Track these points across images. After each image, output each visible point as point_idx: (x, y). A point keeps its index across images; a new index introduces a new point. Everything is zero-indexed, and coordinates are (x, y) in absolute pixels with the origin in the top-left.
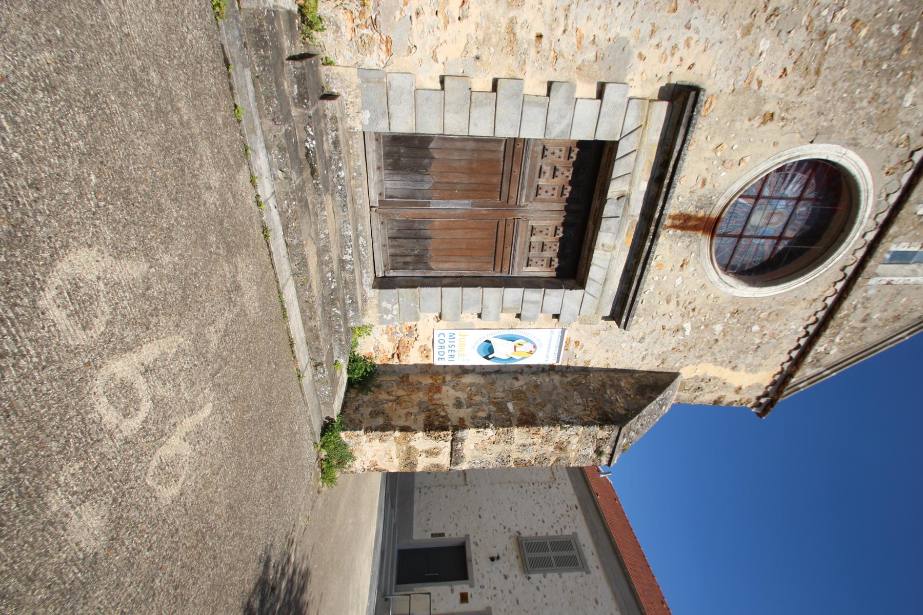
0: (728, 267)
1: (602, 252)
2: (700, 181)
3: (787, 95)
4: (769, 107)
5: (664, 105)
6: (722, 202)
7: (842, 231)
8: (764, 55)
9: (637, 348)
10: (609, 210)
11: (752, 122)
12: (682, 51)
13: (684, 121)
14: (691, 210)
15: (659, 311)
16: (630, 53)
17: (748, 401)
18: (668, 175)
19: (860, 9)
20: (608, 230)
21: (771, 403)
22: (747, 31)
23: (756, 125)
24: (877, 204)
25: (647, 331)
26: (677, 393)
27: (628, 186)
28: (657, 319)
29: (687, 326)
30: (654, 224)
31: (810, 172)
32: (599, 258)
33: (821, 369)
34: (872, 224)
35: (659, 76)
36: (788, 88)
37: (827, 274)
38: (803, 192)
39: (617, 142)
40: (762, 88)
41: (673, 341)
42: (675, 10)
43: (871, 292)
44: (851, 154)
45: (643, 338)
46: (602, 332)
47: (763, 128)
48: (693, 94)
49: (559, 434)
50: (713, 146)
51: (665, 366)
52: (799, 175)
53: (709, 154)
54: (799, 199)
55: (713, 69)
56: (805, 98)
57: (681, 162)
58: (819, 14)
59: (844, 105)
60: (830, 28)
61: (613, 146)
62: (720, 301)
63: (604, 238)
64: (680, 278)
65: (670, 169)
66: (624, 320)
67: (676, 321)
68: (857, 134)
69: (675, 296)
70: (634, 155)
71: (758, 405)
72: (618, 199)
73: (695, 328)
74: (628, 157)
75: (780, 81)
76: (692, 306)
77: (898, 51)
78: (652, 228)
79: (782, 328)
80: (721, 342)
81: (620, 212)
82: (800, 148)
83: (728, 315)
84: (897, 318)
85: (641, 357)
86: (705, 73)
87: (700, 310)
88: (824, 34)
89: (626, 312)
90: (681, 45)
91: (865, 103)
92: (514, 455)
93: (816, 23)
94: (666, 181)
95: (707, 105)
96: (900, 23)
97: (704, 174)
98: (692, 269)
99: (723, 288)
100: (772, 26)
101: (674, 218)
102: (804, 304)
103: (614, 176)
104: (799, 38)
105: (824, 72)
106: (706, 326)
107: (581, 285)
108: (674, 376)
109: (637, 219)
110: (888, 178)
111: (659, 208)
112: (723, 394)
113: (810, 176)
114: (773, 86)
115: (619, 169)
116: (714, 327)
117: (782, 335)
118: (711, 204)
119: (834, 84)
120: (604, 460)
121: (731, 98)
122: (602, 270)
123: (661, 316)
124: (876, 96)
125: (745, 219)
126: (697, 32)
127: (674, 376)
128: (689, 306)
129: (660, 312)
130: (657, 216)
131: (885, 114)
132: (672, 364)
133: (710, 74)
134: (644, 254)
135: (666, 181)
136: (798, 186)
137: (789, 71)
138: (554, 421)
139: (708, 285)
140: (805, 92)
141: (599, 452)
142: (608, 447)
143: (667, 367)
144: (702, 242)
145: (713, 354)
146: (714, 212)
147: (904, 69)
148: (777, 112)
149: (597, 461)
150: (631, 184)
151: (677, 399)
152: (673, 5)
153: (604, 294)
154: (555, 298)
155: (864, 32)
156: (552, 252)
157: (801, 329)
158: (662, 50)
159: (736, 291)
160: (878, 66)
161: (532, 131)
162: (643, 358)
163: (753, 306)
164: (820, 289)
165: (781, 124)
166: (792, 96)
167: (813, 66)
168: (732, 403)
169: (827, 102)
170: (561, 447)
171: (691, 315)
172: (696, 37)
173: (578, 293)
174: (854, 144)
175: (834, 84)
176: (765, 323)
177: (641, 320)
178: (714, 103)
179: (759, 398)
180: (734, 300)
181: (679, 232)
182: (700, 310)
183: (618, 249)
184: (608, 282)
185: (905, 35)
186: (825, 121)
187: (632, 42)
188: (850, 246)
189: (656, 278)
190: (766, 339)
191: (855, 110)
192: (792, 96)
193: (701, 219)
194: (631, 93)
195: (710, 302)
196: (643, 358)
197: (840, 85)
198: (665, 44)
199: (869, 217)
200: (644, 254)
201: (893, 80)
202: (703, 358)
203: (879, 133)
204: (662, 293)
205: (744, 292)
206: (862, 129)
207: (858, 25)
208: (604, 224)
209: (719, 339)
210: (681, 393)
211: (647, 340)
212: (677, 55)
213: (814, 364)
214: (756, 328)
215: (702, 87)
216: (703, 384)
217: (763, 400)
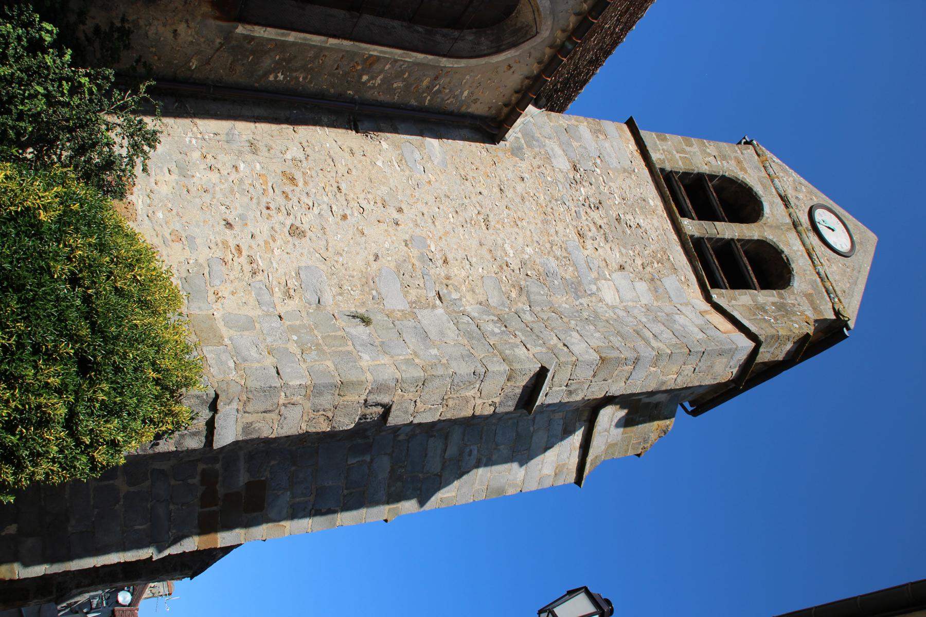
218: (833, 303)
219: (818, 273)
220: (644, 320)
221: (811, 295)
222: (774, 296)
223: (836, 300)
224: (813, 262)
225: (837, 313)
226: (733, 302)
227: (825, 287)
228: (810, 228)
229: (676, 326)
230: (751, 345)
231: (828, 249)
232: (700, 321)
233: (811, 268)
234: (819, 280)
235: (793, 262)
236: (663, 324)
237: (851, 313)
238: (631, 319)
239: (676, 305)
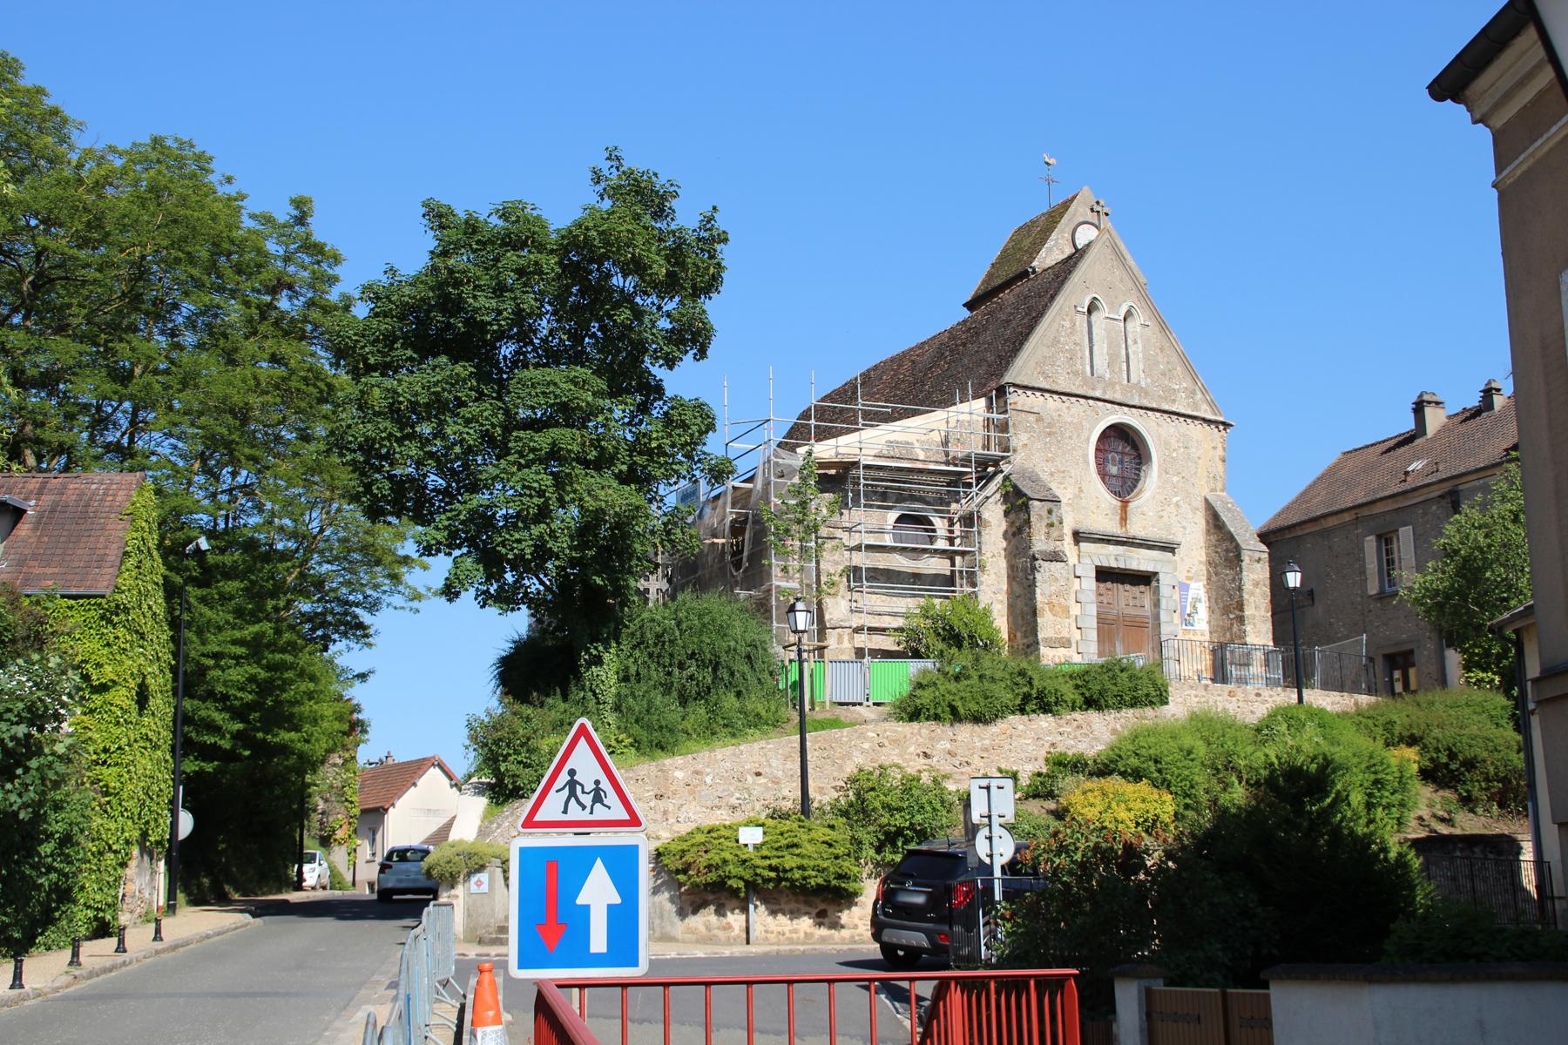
10: (1123, 566)
21: (1223, 423)
24: (1112, 413)
49: (1248, 586)
61: (1097, 568)
67: (1172, 509)
73: (1176, 494)
77: (1054, 433)
84: (1162, 350)
92: (1263, 613)
108: (1206, 500)
115: (1105, 564)
127: (1206, 500)
138: (1240, 589)
143: (1201, 505)
151: (1222, 490)
154: (1165, 590)
156: (1136, 590)
161: (1093, 610)
166: (1073, 481)
170: (1256, 584)
173: (1161, 576)
174: (1088, 439)
185: (1050, 434)
192: (1073, 481)
211: (1184, 524)
213: (1196, 407)
217: (1221, 427)
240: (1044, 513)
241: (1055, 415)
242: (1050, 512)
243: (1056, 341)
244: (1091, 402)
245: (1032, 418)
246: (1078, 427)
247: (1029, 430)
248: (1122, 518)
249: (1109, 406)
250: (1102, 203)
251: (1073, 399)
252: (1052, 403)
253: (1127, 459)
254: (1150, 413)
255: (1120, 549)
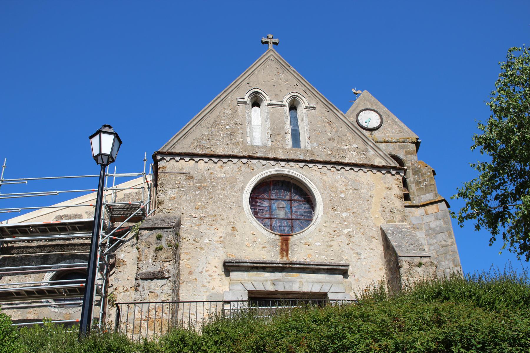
0: (309, 220)
1: (304, 287)
2: (264, 249)
3: (224, 225)
4: (230, 230)
5: (231, 274)
6: (273, 236)
7: (282, 176)
8: (210, 239)
9: (365, 255)
11: (236, 235)
12: (211, 273)
13: (237, 265)
14: (278, 249)
15: (338, 249)
16: (212, 294)
17: (397, 180)
18: (261, 265)
19: (192, 208)
20: (291, 286)
22: (202, 249)
23: (237, 233)
24: (268, 168)
25: (352, 252)
26: (397, 223)
27: (268, 282)
28: (343, 249)
29: (346, 231)
30: (285, 266)
31: (256, 200)
32: (307, 288)
33: (368, 147)
34: (277, 166)
35: (220, 279)
36: (222, 225)
37: (305, 173)
38: (266, 199)
39: (248, 291)
40: (222, 236)
41: (357, 236)
42: (196, 279)
43: (315, 144)
44: (246, 189)
45: (357, 253)
46: (356, 277)
47: (238, 230)
48: (227, 264)
50: (247, 249)
51: (376, 236)
52: (258, 204)
53: (251, 249)
54: (270, 199)
55: (216, 258)
56: (225, 218)
57: (255, 262)
58: (194, 223)
59: (227, 200)
60: (199, 217)
61: (250, 293)
62: (327, 219)
63: (295, 288)
64: (316, 244)
65: (258, 265)
66: (343, 268)
68: (238, 190)
69: (327, 243)
70: (253, 283)
71: (398, 173)
72: (274, 285)
73: (347, 227)
74: (255, 285)
75: (219, 230)
76: (333, 233)
77: (205, 188)
78: (287, 266)
79: (340, 182)
80: (354, 210)
81: (281, 283)
82: (245, 211)
83: (336, 212)
84: (330, 123)
85: (371, 251)
86: (218, 261)
87: (334, 228)
88: (201, 219)
89: (337, 268)
90: (208, 273)
91: (225, 192)
93: (198, 223)
94: (264, 265)
95: (231, 256)
96: (195, 192)
97: (261, 248)
98: (310, 240)
99: (319, 220)
100: (199, 239)
101: (282, 256)
102: (324, 177)
103: (264, 290)
104: (203, 228)
105: (215, 213)
106: (345, 221)
107: (325, 294)
108: (381, 229)
109: (284, 273)
110: (255, 169)
111: (277, 265)
112: (393, 196)
113: (258, 199)
114: (221, 232)
115: (260, 288)
116: (344, 217)
117: (345, 180)
118: (274, 241)
119: (219, 207)
120: (424, 260)
121: (227, 247)
122: (314, 285)
123: (341, 247)
124: (223, 189)
125: (282, 221)
126: (203, 268)
127: (381, 229)
128: (333, 234)
129: (338, 248)
130: (281, 265)
131: (229, 182)
132: (375, 232)
133: (219, 259)
134: (302, 266)
135: (264, 265)
136: (263, 202)
137: (215, 227)
139: (318, 229)
140: (223, 218)
141: (420, 265)
142: (415, 260)
144: (294, 239)
145: (364, 211)
146: (278, 238)
147: (211, 183)
148: (232, 226)
149: (427, 264)
150: (266, 281)
152: (194, 280)
153: (329, 281)
155: (200, 204)
157: (340, 172)
158: (210, 281)
159: (320, 214)
160: (211, 193)
162: (372, 249)
163: (328, 202)
164: (314, 173)
165: (236, 223)
166: (225, 223)
167: (213, 218)
168: (400, 189)
169: (226, 207)
171: (338, 231)
172: (205, 268)
174: (242, 189)
175: (219, 207)
176: (338, 192)
177: (345, 258)
178: (229, 254)
179: (393, 175)
180: (326, 212)
181: (289, 252)
182: (334, 228)
183: (301, 280)
184: (321, 281)
185: (199, 188)
186: (233, 205)
187: (208, 294)
188: (289, 170)
189: (317, 256)
190: (349, 187)
191: (228, 195)
192: (225, 223)
193: (282, 244)
194: (228, 290)
195: (328, 224)
196: (372, 249)
197: (219, 205)
198: (208, 280)
199: (274, 168)
200: (302, 266)
201: (216, 185)
202: (367, 216)
203: (237, 181)
204: (326, 251)
205: (320, 209)
206: (236, 189)
207: (197, 207)
208: (288, 289)
209: (352, 212)
210: (397, 220)
212: (212, 274)
214: (342, 195)
215: (223, 261)
216: (388, 210)
217: (393, 172)
218: (409, 142)
219: (395, 142)
220: (435, 241)
221: (406, 152)
222: (409, 172)
223: (408, 140)
224: (390, 142)
225: (413, 143)
226: (415, 194)
227: (401, 142)
228: (370, 132)
229: (438, 229)
230: (444, 202)
231: (380, 128)
232: (433, 218)
233: (393, 144)
234: (398, 143)
235: (391, 153)
236: (436, 234)
237: (414, 136)
238: (435, 245)
239: (424, 223)
240: (153, 239)
241: (207, 174)
242: (159, 238)
243: (216, 124)
244: (244, 161)
245: (182, 178)
246: (231, 181)
247: (178, 186)
248: (282, 250)
249: (264, 162)
250: (270, 36)
251: (225, 160)
252: (203, 165)
253: (295, 205)
254: (311, 165)
255: (278, 275)
